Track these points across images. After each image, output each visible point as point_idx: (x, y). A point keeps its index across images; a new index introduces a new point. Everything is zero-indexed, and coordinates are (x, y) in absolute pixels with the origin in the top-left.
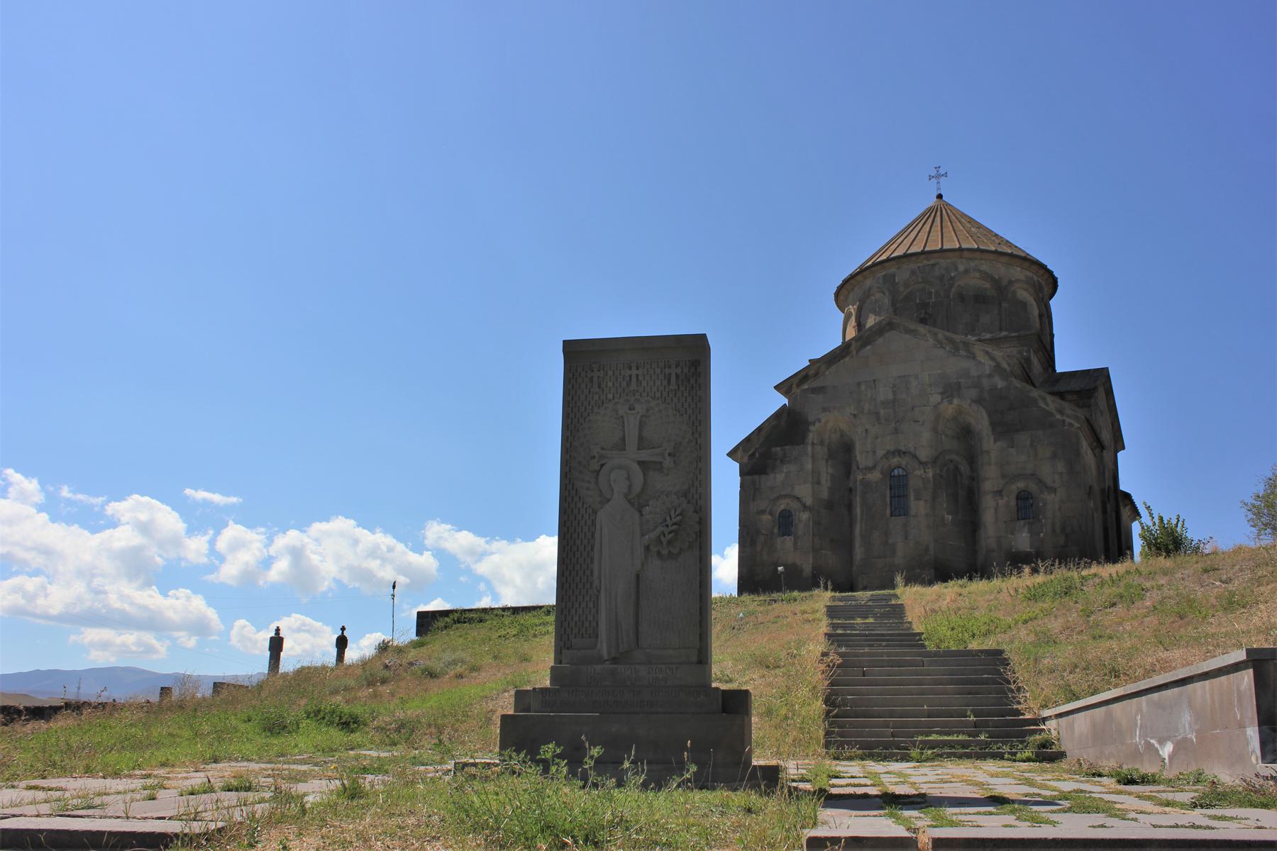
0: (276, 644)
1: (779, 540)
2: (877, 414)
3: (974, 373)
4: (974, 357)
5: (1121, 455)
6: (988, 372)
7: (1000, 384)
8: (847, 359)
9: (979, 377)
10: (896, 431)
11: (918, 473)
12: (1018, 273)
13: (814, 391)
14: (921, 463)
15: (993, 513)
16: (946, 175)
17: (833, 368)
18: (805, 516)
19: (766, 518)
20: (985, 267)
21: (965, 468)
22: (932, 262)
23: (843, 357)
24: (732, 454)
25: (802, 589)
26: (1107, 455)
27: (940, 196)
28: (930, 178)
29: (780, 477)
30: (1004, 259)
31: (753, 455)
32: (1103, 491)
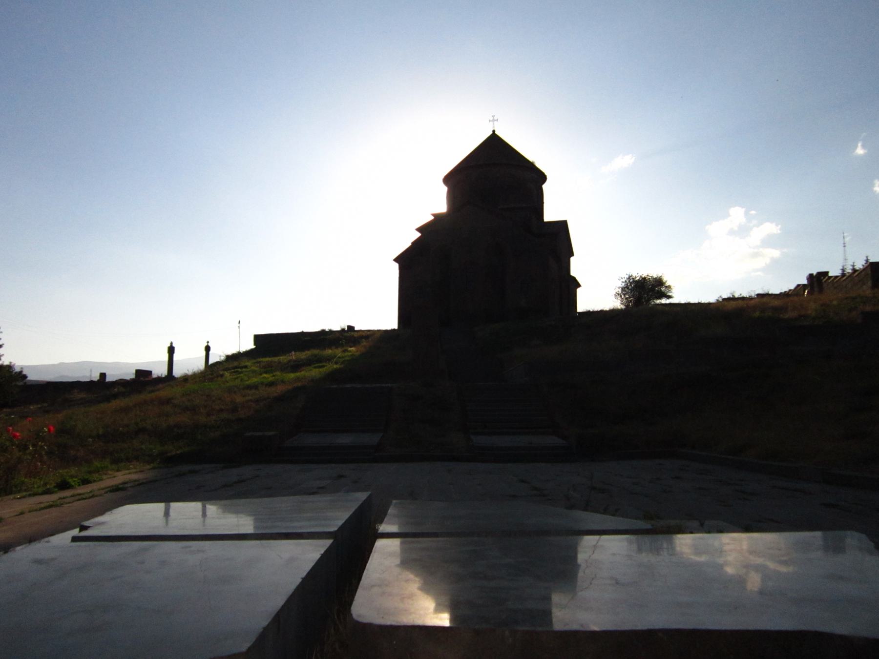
0: (171, 350)
5: (572, 259)
24: (396, 260)
27: (494, 131)
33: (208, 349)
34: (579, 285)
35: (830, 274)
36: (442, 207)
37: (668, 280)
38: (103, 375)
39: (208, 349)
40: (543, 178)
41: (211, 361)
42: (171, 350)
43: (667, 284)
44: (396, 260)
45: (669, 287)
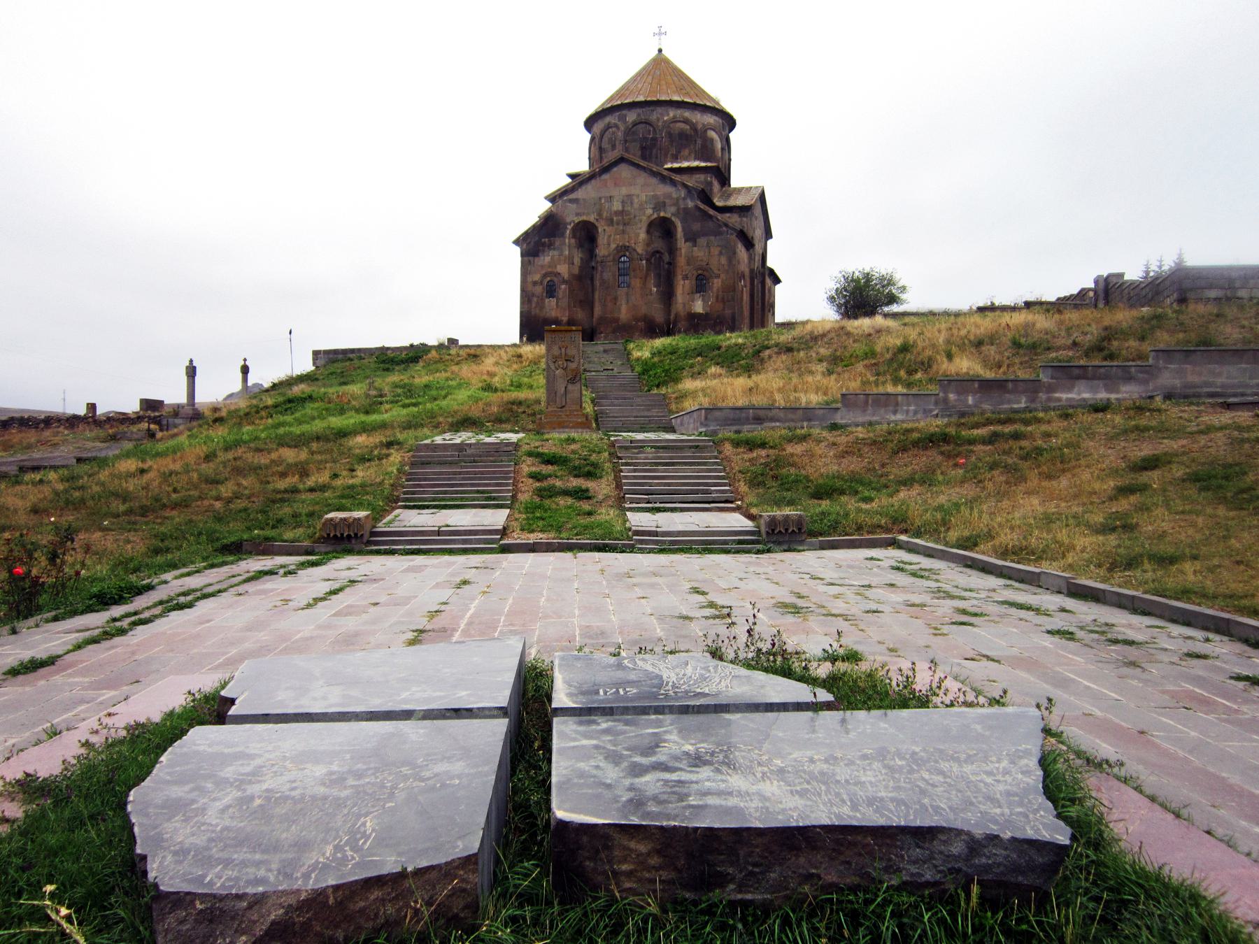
0: (191, 372)
2: (612, 220)
3: (674, 195)
5: (769, 242)
7: (690, 204)
9: (678, 199)
10: (623, 232)
12: (710, 119)
13: (571, 201)
15: (682, 287)
21: (666, 258)
24: (517, 242)
26: (758, 248)
27: (660, 51)
28: (654, 34)
29: (548, 259)
32: (752, 271)
33: (245, 370)
34: (777, 280)
35: (1126, 278)
36: (583, 166)
37: (902, 278)
38: (92, 407)
39: (245, 370)
40: (730, 122)
41: (250, 384)
42: (191, 372)
43: (900, 284)
44: (517, 242)
45: (903, 289)
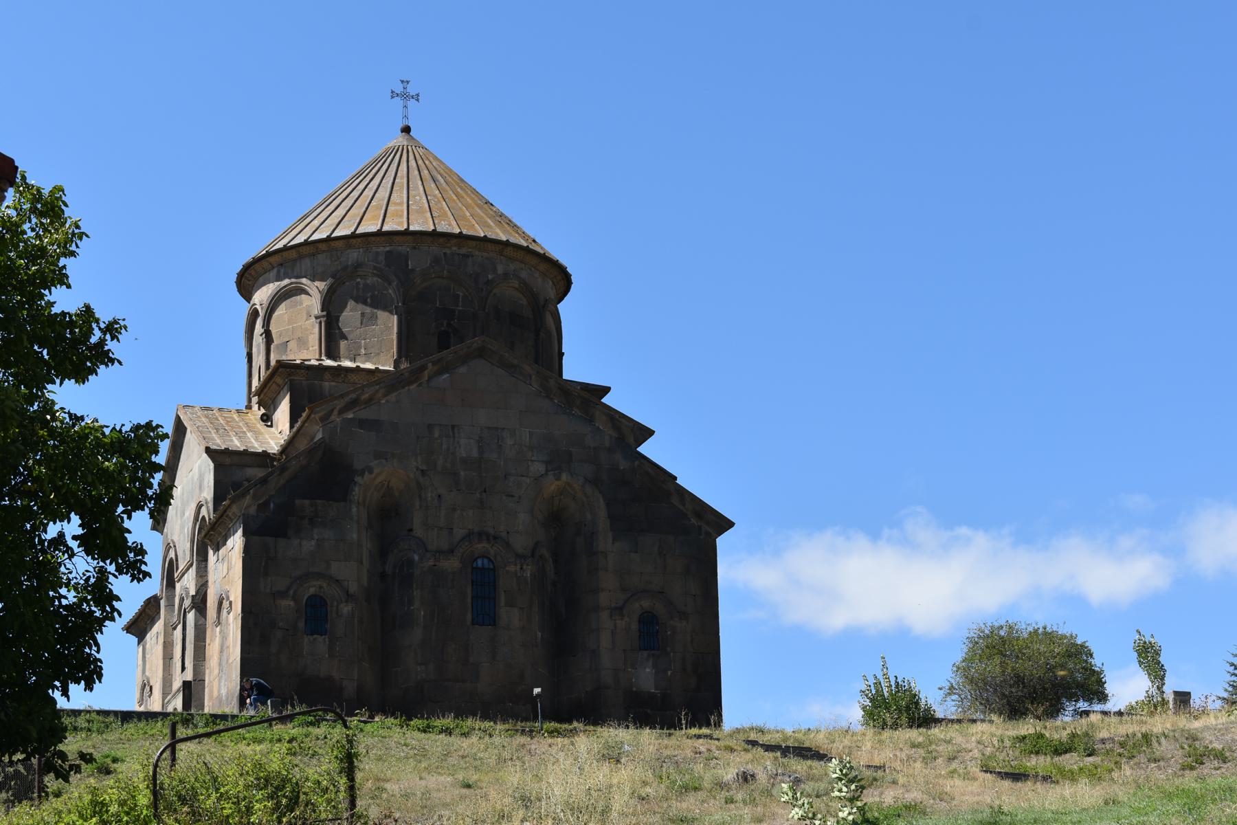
1: (306, 640)
4: (590, 420)
6: (607, 444)
8: (413, 387)
11: (512, 568)
13: (362, 423)
14: (518, 556)
16: (417, 97)
17: (393, 397)
18: (346, 609)
19: (287, 603)
20: (524, 274)
22: (464, 251)
23: (411, 383)
25: (560, 721)
27: (406, 130)
28: (394, 94)
29: (308, 546)
30: (543, 267)
31: (266, 504)
